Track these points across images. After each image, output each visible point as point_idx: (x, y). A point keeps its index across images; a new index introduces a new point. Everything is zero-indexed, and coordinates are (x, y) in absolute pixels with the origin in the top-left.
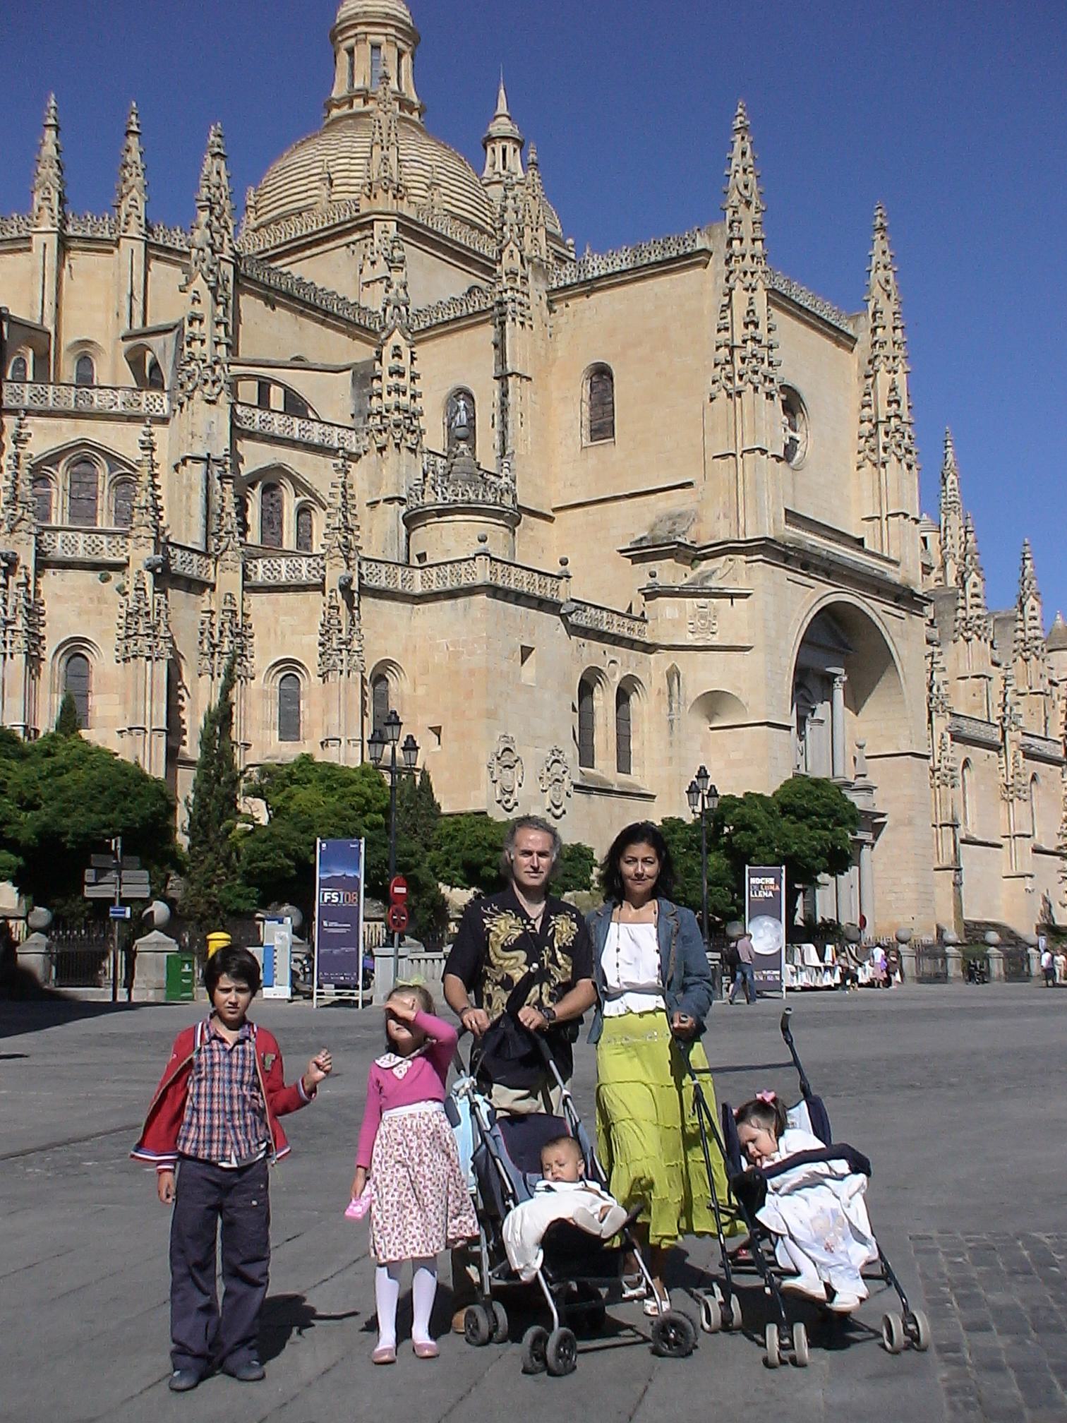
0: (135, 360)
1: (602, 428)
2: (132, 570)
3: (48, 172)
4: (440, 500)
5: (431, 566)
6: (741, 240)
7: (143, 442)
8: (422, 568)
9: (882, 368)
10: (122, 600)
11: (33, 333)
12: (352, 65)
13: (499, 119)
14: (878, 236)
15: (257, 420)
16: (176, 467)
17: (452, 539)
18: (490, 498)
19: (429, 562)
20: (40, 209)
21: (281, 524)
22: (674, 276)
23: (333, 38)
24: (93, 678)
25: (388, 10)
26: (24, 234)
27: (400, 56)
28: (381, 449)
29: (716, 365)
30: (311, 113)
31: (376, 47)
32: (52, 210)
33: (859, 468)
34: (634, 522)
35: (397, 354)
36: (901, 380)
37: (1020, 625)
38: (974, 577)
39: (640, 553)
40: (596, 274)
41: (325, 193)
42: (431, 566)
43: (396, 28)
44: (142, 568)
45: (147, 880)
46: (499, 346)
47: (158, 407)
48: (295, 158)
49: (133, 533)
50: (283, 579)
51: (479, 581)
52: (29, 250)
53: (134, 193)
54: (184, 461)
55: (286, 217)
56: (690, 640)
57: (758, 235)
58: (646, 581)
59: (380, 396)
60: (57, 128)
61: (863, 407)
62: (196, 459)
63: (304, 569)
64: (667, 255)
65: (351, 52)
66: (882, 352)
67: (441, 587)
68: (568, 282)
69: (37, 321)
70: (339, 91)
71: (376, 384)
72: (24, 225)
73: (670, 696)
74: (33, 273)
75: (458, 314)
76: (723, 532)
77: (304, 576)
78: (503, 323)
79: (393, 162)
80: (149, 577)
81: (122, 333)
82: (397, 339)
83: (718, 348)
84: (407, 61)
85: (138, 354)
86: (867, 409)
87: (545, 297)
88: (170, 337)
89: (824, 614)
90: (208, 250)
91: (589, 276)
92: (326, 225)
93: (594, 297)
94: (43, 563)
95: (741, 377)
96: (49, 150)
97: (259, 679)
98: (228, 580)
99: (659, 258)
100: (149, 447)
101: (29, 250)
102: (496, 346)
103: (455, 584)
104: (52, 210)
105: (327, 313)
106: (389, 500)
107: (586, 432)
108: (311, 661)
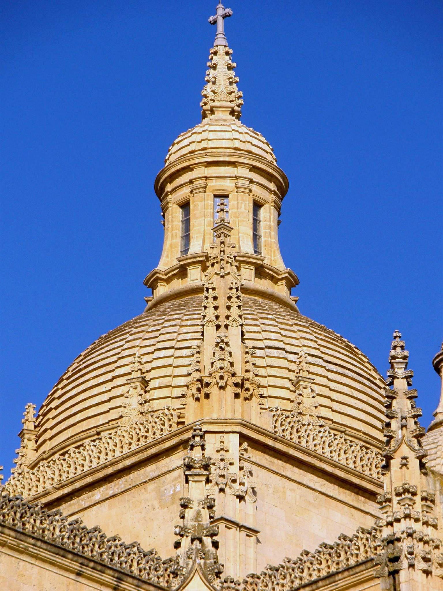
12: (186, 222)
23: (160, 191)
25: (237, 144)
27: (257, 206)
43: (254, 169)
48: (95, 357)
65: (185, 206)
70: (168, 260)
78: (394, 573)
79: (235, 345)
84: (268, 214)
92: (134, 447)
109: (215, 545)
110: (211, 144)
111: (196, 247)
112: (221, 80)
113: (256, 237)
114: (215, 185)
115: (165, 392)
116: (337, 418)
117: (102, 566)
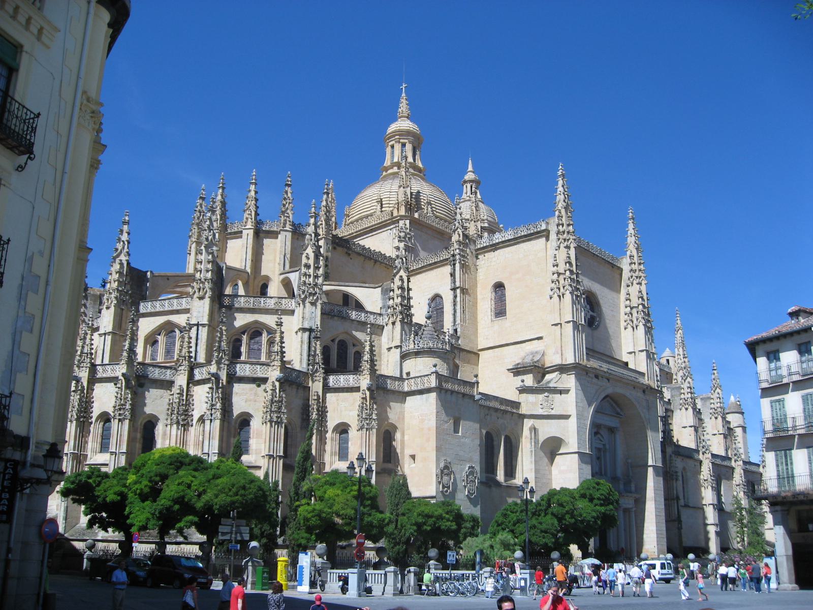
0: (287, 284)
1: (500, 311)
2: (270, 381)
4: (416, 347)
5: (412, 378)
6: (563, 225)
7: (277, 322)
8: (407, 379)
9: (635, 282)
10: (265, 394)
11: (240, 273)
13: (469, 173)
14: (631, 222)
15: (336, 311)
16: (296, 332)
18: (440, 346)
19: (412, 376)
20: (247, 218)
21: (346, 358)
22: (533, 242)
24: (252, 431)
26: (240, 230)
28: (394, 323)
29: (553, 282)
30: (373, 172)
31: (404, 145)
32: (252, 219)
33: (625, 329)
34: (515, 356)
35: (401, 279)
37: (712, 401)
38: (689, 379)
39: (518, 371)
40: (497, 241)
41: (379, 207)
42: (412, 378)
44: (274, 380)
45: (248, 531)
46: (453, 275)
47: (290, 305)
49: (272, 364)
50: (341, 385)
52: (241, 237)
53: (288, 211)
54: (300, 329)
55: (361, 219)
56: (540, 412)
57: (571, 223)
58: (520, 384)
59: (393, 299)
60: (256, 184)
61: (627, 300)
62: (304, 330)
63: (351, 380)
64: (529, 232)
65: (392, 147)
66: (634, 275)
67: (416, 388)
68: (485, 245)
69: (243, 268)
70: (387, 163)
71: (391, 293)
72: (240, 226)
73: (531, 439)
74: (243, 247)
75: (436, 260)
78: (454, 265)
80: (277, 384)
81: (280, 272)
82: (402, 273)
83: (553, 274)
85: (286, 281)
86: (628, 301)
87: (474, 252)
88: (298, 272)
89: (608, 399)
90: (313, 235)
91: (494, 242)
93: (497, 252)
94: (233, 378)
95: (564, 287)
96: (253, 193)
97: (330, 432)
98: (316, 387)
99: (526, 233)
100: (280, 324)
101: (241, 237)
102: (451, 275)
103: (422, 387)
104: (252, 219)
105: (376, 261)
106: (396, 347)
108: (354, 423)
110: (401, 128)
111: (396, 160)
112: (403, 107)
113: (414, 160)
114: (401, 141)
115: (388, 205)
116: (437, 214)
117: (370, 259)
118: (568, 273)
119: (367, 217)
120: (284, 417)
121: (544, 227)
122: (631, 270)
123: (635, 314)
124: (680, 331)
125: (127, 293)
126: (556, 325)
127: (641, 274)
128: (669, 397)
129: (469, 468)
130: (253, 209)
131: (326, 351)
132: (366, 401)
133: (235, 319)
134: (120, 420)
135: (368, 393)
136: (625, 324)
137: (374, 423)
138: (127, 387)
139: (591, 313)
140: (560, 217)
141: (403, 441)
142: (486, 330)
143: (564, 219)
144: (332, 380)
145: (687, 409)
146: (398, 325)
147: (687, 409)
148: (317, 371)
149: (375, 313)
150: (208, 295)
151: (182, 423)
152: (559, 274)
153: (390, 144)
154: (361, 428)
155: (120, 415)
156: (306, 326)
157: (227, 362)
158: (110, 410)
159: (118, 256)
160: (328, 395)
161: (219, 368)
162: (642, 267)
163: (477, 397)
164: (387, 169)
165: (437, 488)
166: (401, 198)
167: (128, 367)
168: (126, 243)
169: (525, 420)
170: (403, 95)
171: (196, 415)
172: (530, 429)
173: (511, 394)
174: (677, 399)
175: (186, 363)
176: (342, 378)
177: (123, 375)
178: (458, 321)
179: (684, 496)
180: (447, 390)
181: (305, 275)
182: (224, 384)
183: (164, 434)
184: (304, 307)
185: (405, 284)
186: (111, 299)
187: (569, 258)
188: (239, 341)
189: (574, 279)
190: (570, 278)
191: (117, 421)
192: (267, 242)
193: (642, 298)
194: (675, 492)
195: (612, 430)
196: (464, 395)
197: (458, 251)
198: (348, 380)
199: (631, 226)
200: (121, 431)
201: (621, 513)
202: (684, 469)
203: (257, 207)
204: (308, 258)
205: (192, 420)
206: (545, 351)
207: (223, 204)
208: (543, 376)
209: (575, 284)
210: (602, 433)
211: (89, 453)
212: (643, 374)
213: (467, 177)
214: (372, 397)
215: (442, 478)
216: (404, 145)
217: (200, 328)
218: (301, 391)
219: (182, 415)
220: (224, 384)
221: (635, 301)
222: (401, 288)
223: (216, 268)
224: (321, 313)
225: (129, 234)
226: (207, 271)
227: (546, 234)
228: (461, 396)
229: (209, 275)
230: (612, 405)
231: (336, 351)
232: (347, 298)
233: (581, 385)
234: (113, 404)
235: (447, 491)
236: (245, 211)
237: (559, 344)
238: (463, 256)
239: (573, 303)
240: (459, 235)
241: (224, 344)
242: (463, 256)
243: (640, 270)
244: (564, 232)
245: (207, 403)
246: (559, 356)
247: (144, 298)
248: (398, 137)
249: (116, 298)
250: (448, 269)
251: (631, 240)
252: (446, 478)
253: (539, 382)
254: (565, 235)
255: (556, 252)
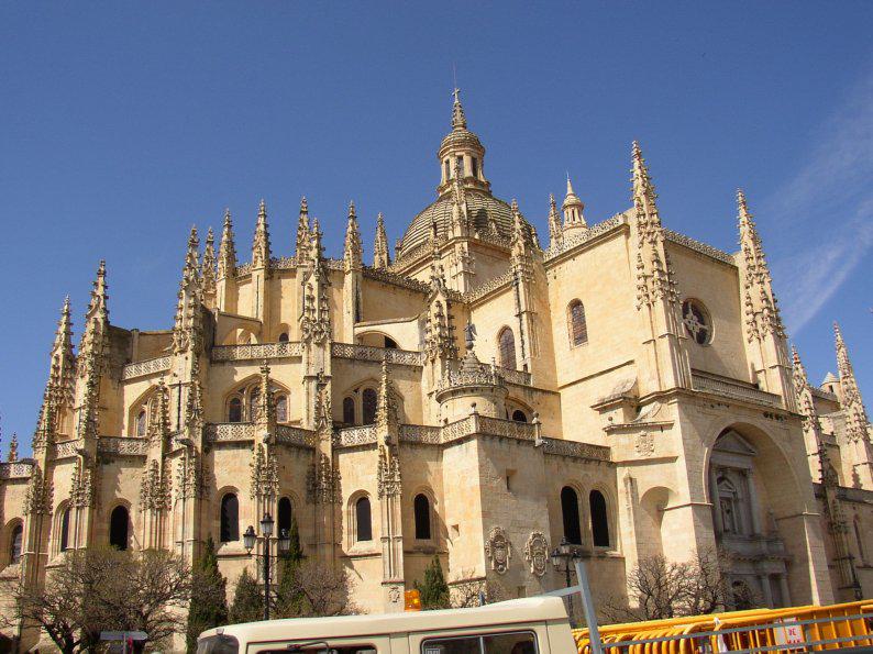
1: (580, 336)
3: (261, 239)
9: (755, 282)
17: (460, 408)
28: (433, 361)
34: (605, 388)
35: (439, 305)
36: (767, 287)
38: (854, 404)
51: (473, 431)
54: (305, 377)
56: (637, 456)
58: (607, 423)
60: (265, 216)
62: (309, 378)
64: (604, 231)
65: (447, 162)
71: (428, 325)
76: (653, 387)
77: (368, 440)
78: (517, 284)
80: (265, 446)
89: (733, 432)
90: (316, 260)
94: (211, 443)
96: (262, 227)
98: (326, 447)
100: (268, 371)
101: (250, 282)
107: (572, 341)
109: (444, 281)
114: (458, 154)
118: (656, 274)
119: (419, 246)
120: (276, 489)
121: (621, 222)
122: (749, 267)
123: (760, 322)
124: (842, 349)
125: (105, 357)
126: (649, 342)
127: (761, 270)
128: (832, 430)
129: (534, 536)
130: (262, 245)
131: (348, 403)
132: (385, 459)
133: (236, 373)
134: (78, 508)
135: (387, 448)
136: (749, 336)
137: (398, 488)
138: (86, 467)
139: (700, 326)
140: (640, 206)
141: (443, 508)
142: (567, 362)
143: (645, 208)
144: (346, 438)
145: (856, 442)
146: (438, 362)
147: (856, 442)
148: (323, 427)
149: (410, 352)
150: (189, 348)
151: (157, 507)
152: (646, 277)
153: (445, 159)
154: (381, 495)
155: (78, 501)
156: (313, 373)
157: (201, 425)
158: (68, 496)
159: (93, 313)
160: (343, 458)
161: (192, 433)
162: (762, 261)
163: (538, 442)
164: (443, 189)
165: (487, 566)
166: (455, 216)
167: (86, 441)
168: (102, 297)
169: (618, 469)
170: (457, 102)
171: (173, 493)
172: (625, 480)
173: (600, 439)
174: (843, 430)
175: (160, 432)
176: (356, 433)
177: (80, 452)
178: (528, 355)
179: (861, 554)
180: (493, 437)
181: (308, 309)
182: (200, 451)
183: (139, 523)
184: (309, 349)
185: (445, 312)
186: (85, 365)
187: (656, 255)
188: (237, 401)
189: (665, 281)
190: (659, 279)
191: (74, 510)
192: (284, 282)
193: (767, 300)
194: (846, 548)
195: (743, 473)
196: (519, 441)
197: (519, 267)
198: (363, 436)
199: (742, 212)
200: (81, 520)
201: (766, 581)
202: (856, 517)
203: (268, 244)
204: (311, 289)
205: (170, 503)
206: (641, 379)
207: (231, 244)
208: (638, 409)
209: (669, 284)
210: (730, 478)
211: (49, 553)
212: (777, 397)
213: (566, 202)
214: (392, 453)
215: (493, 552)
216: (460, 158)
217: (183, 388)
218: (303, 457)
219: (157, 496)
220: (200, 451)
221: (758, 305)
222: (439, 315)
223: (200, 315)
224: (332, 357)
225: (105, 287)
226: (189, 318)
227: (625, 230)
228: (515, 442)
229: (191, 323)
230: (739, 442)
231: (361, 403)
232: (390, 344)
233: (688, 416)
234: (70, 489)
235: (502, 570)
236: (253, 249)
237: (654, 367)
238: (528, 273)
239: (667, 310)
240: (520, 249)
241: (197, 402)
242: (528, 273)
243: (760, 266)
244: (646, 224)
245: (178, 477)
246: (656, 381)
247: (129, 362)
248: (452, 150)
249: (91, 363)
250: (511, 295)
251: (744, 230)
252: (499, 552)
253: (634, 418)
254: (648, 228)
255: (640, 251)
